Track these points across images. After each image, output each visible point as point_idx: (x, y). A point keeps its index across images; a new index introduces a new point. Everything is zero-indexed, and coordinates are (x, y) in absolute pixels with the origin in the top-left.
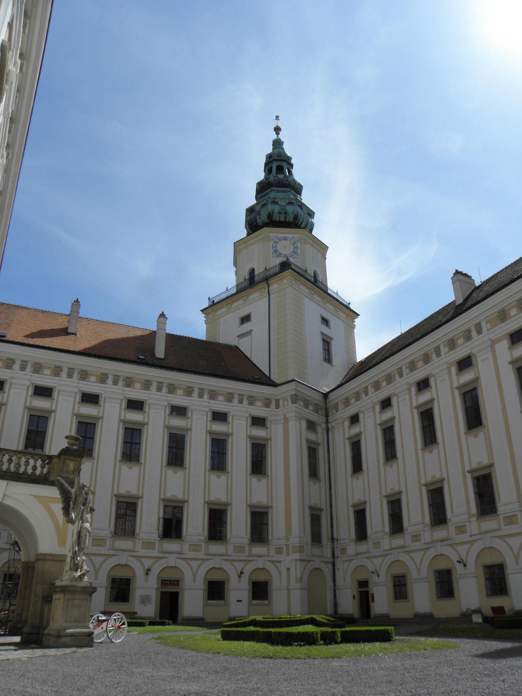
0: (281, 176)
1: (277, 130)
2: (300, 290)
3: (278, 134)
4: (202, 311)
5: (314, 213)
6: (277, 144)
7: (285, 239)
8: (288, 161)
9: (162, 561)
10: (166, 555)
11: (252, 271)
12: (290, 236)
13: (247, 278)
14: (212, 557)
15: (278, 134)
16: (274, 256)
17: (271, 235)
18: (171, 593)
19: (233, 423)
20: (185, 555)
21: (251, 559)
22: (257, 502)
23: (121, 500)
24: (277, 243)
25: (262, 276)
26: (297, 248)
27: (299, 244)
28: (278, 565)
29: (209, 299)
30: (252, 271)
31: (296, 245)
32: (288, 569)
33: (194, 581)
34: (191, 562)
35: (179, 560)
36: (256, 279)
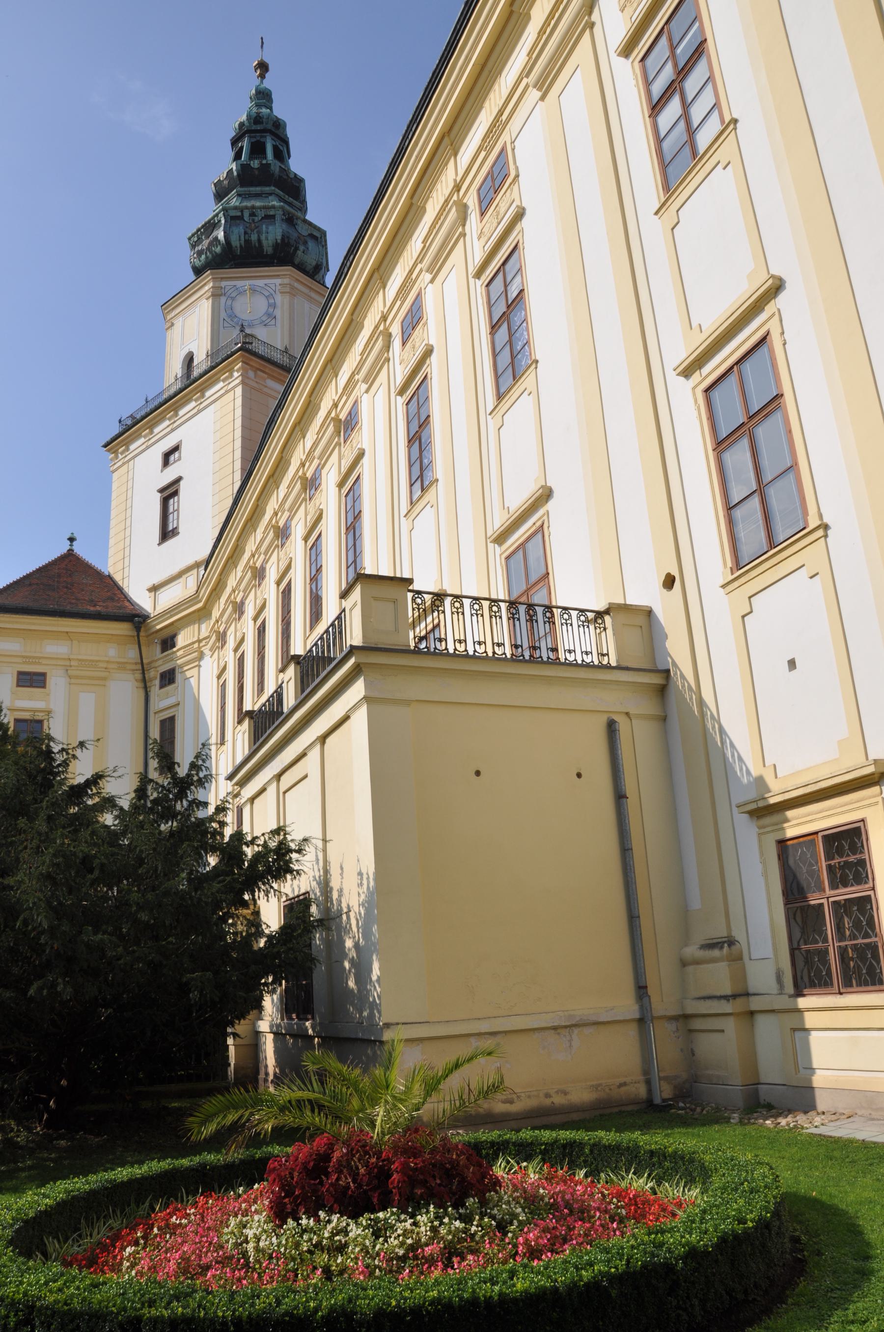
0: (255, 164)
1: (263, 67)
2: (265, 390)
3: (262, 76)
4: (105, 446)
5: (324, 233)
6: (263, 97)
7: (253, 290)
8: (277, 130)
11: (189, 360)
12: (261, 283)
13: (179, 375)
15: (262, 76)
16: (226, 325)
17: (223, 284)
24: (233, 299)
25: (204, 367)
26: (274, 306)
27: (279, 298)
29: (120, 421)
30: (189, 360)
31: (271, 301)
36: (196, 373)
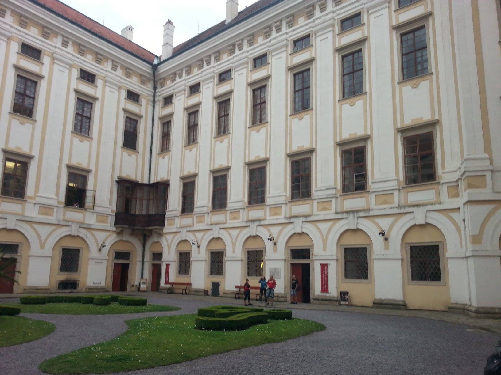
9: (290, 227)
10: (292, 220)
14: (345, 215)
18: (303, 265)
19: (368, 21)
20: (312, 217)
21: (402, 211)
22: (412, 120)
23: (252, 167)
28: (454, 215)
32: (464, 220)
33: (325, 249)
34: (320, 225)
35: (306, 223)
